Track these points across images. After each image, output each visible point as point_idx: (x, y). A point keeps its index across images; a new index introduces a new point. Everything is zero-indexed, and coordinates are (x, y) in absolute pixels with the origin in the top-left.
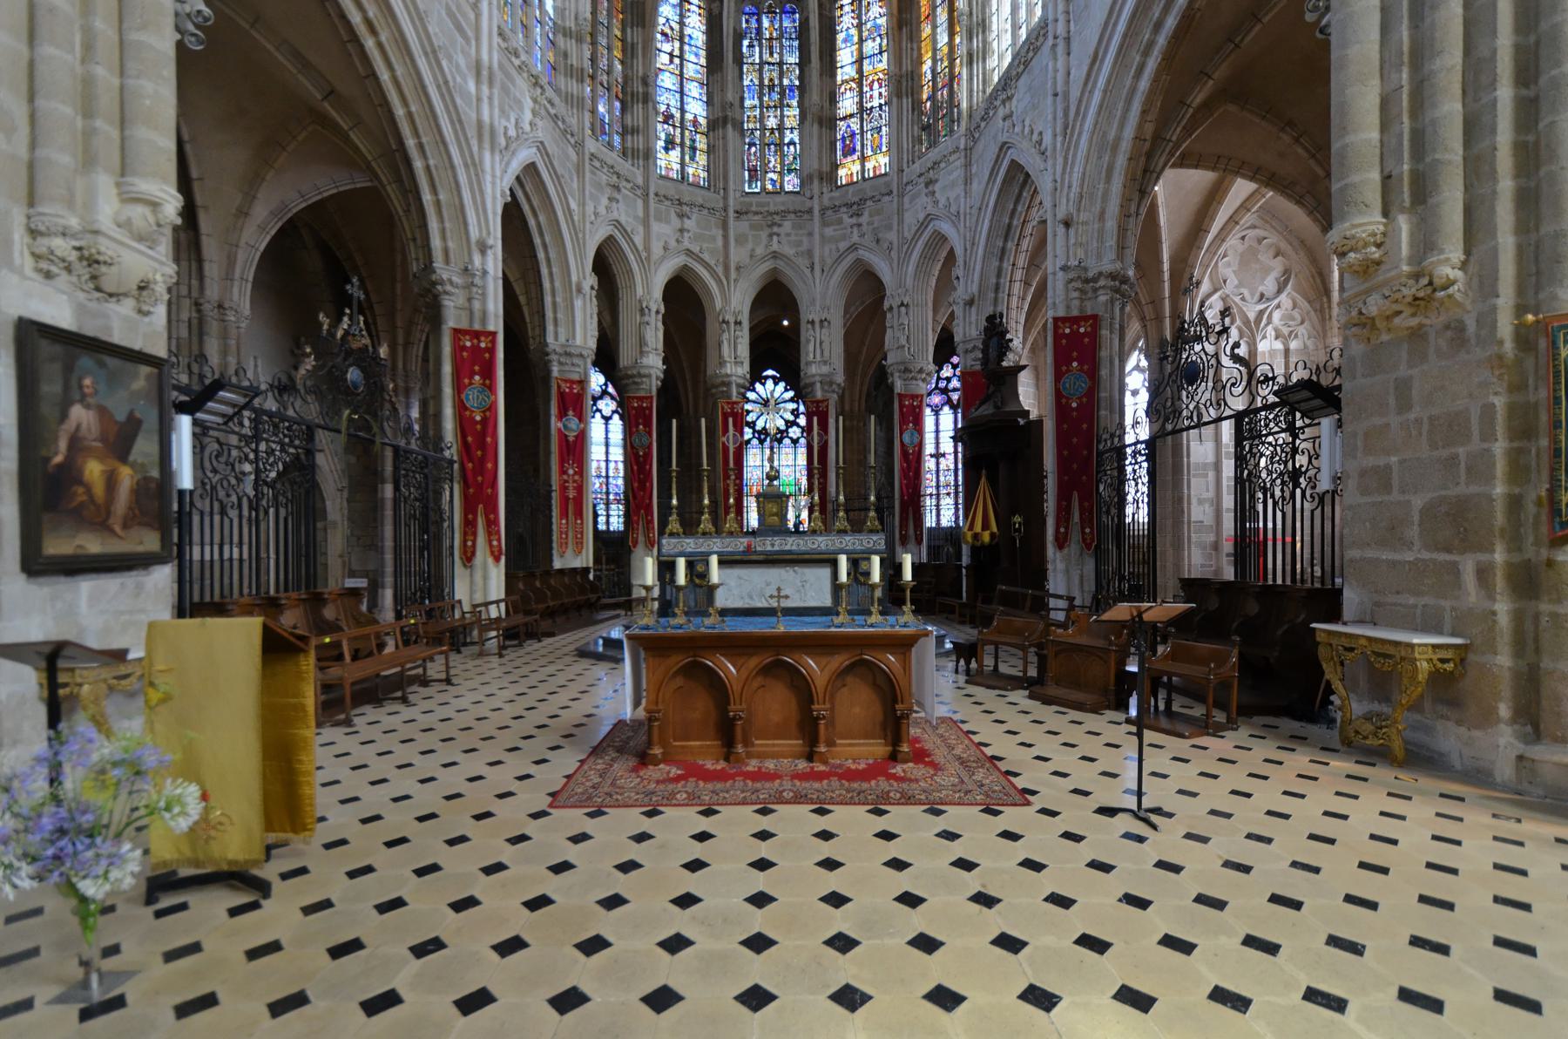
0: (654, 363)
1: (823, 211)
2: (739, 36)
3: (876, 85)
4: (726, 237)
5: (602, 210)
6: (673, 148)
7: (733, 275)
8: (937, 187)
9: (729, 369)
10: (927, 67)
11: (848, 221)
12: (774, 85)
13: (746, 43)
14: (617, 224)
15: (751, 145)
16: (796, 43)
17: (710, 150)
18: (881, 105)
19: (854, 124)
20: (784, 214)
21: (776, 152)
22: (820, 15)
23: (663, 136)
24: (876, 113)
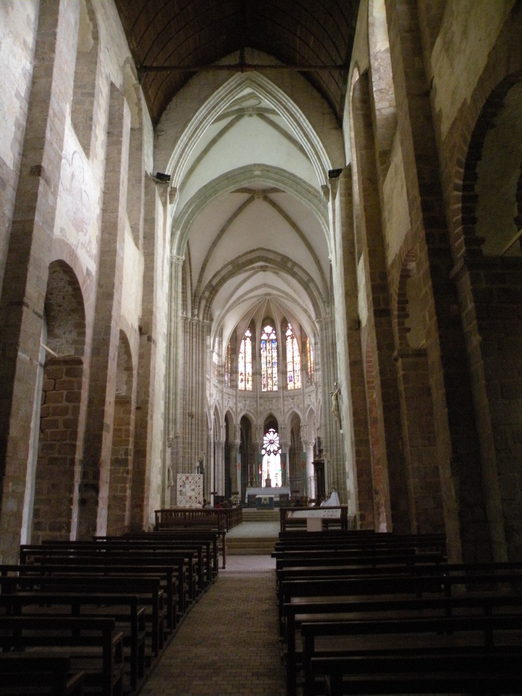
0: (238, 441)
1: (284, 397)
2: (260, 349)
4: (257, 404)
5: (226, 405)
7: (259, 414)
8: (311, 397)
9: (258, 441)
10: (309, 364)
11: (291, 401)
13: (262, 351)
14: (230, 407)
15: (264, 378)
16: (276, 351)
17: (253, 381)
19: (292, 373)
20: (273, 398)
24: (297, 372)
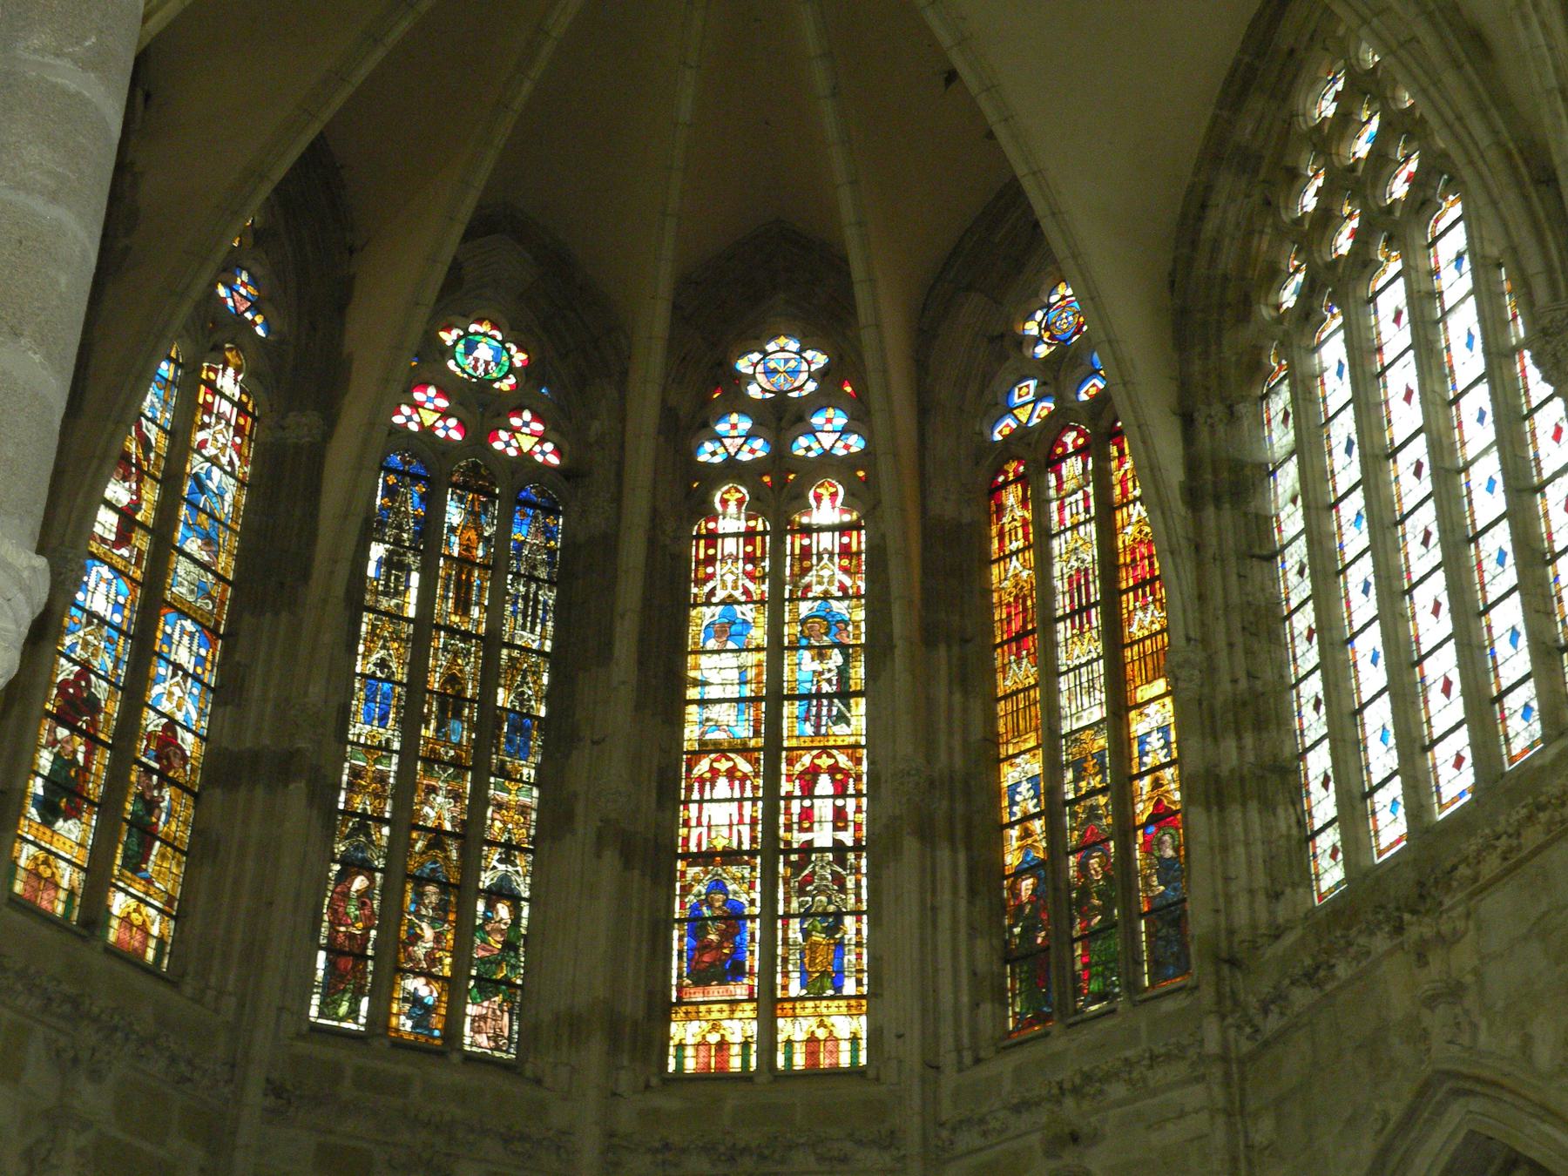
3: (824, 785)
6: (72, 813)
12: (460, 698)
13: (377, 551)
15: (353, 866)
16: (548, 596)
18: (839, 848)
19: (744, 888)
21: (442, 907)
22: (652, 542)
23: (45, 760)
